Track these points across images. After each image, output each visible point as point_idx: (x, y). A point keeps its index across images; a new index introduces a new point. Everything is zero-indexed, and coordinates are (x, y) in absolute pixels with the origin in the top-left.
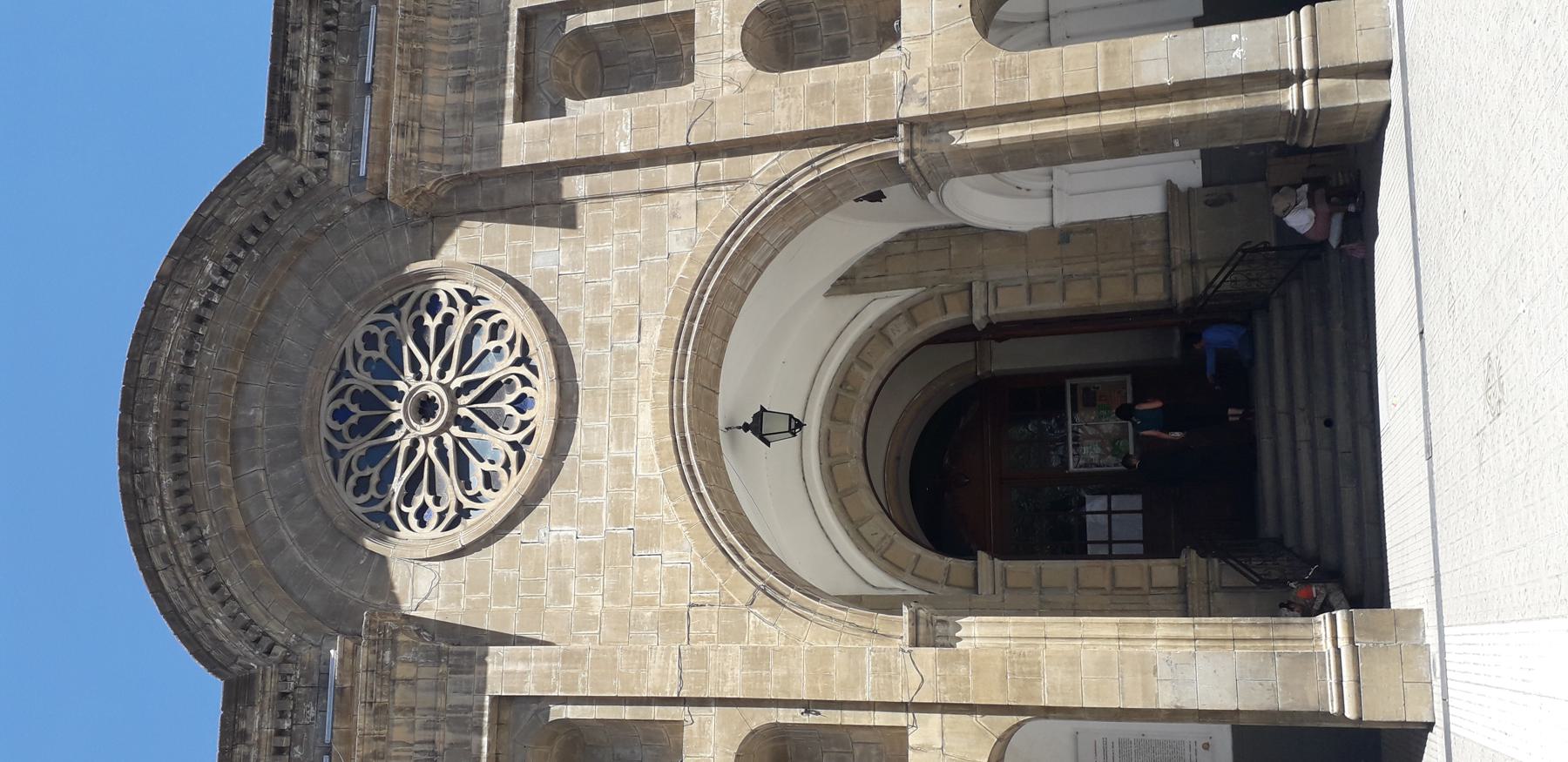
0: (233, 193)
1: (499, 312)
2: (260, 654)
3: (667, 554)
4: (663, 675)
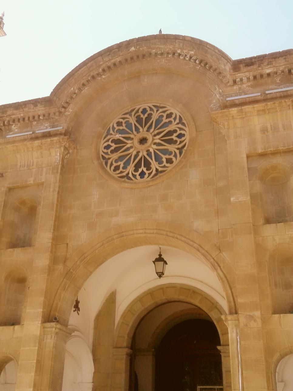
1: (176, 160)
2: (62, 104)
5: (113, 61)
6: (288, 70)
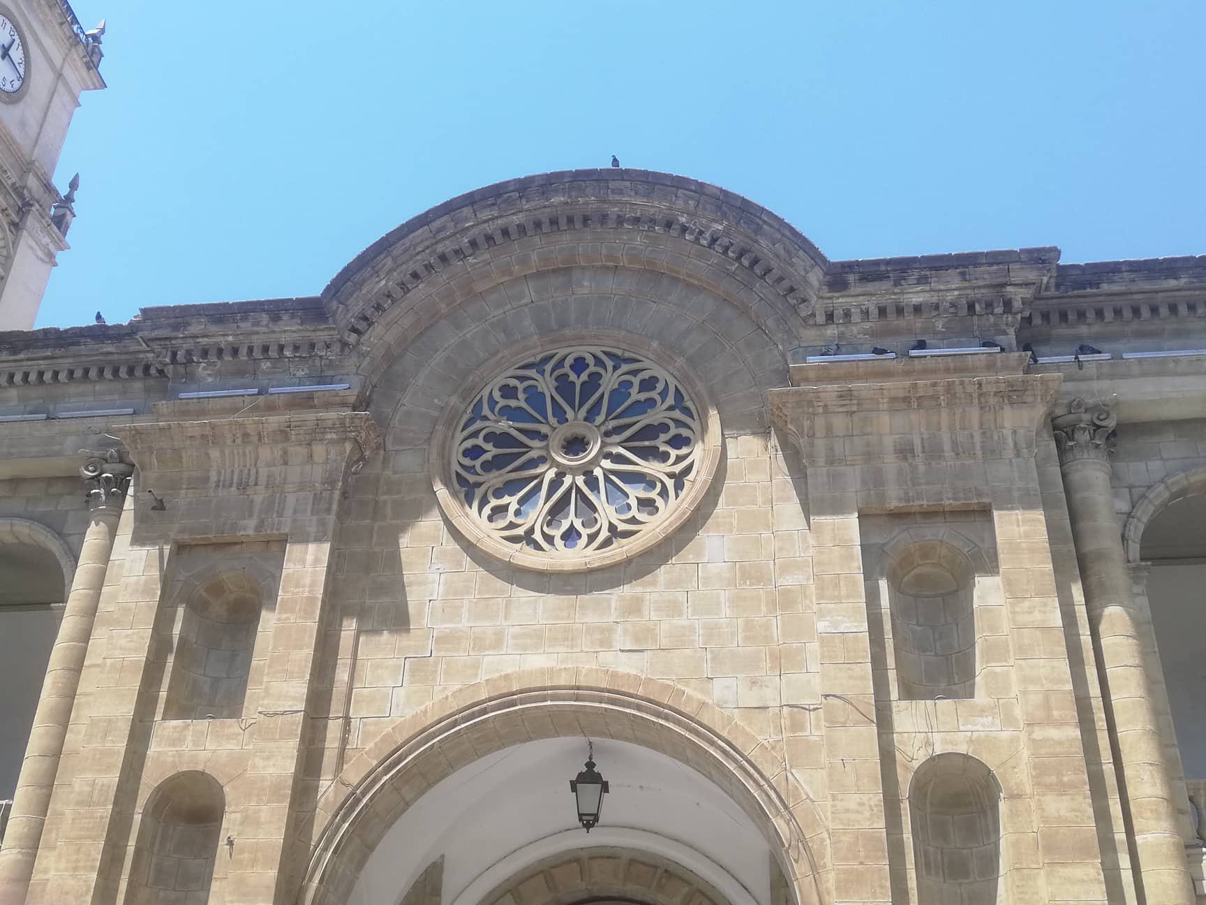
3: (401, 692)
6: (967, 302)
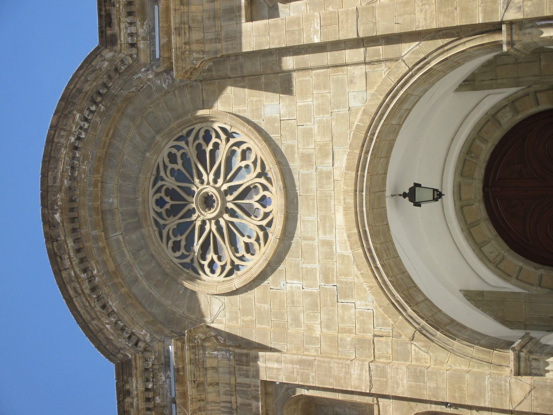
0: (85, 74)
1: (246, 143)
3: (358, 303)
4: (360, 379)
5: (72, 254)
